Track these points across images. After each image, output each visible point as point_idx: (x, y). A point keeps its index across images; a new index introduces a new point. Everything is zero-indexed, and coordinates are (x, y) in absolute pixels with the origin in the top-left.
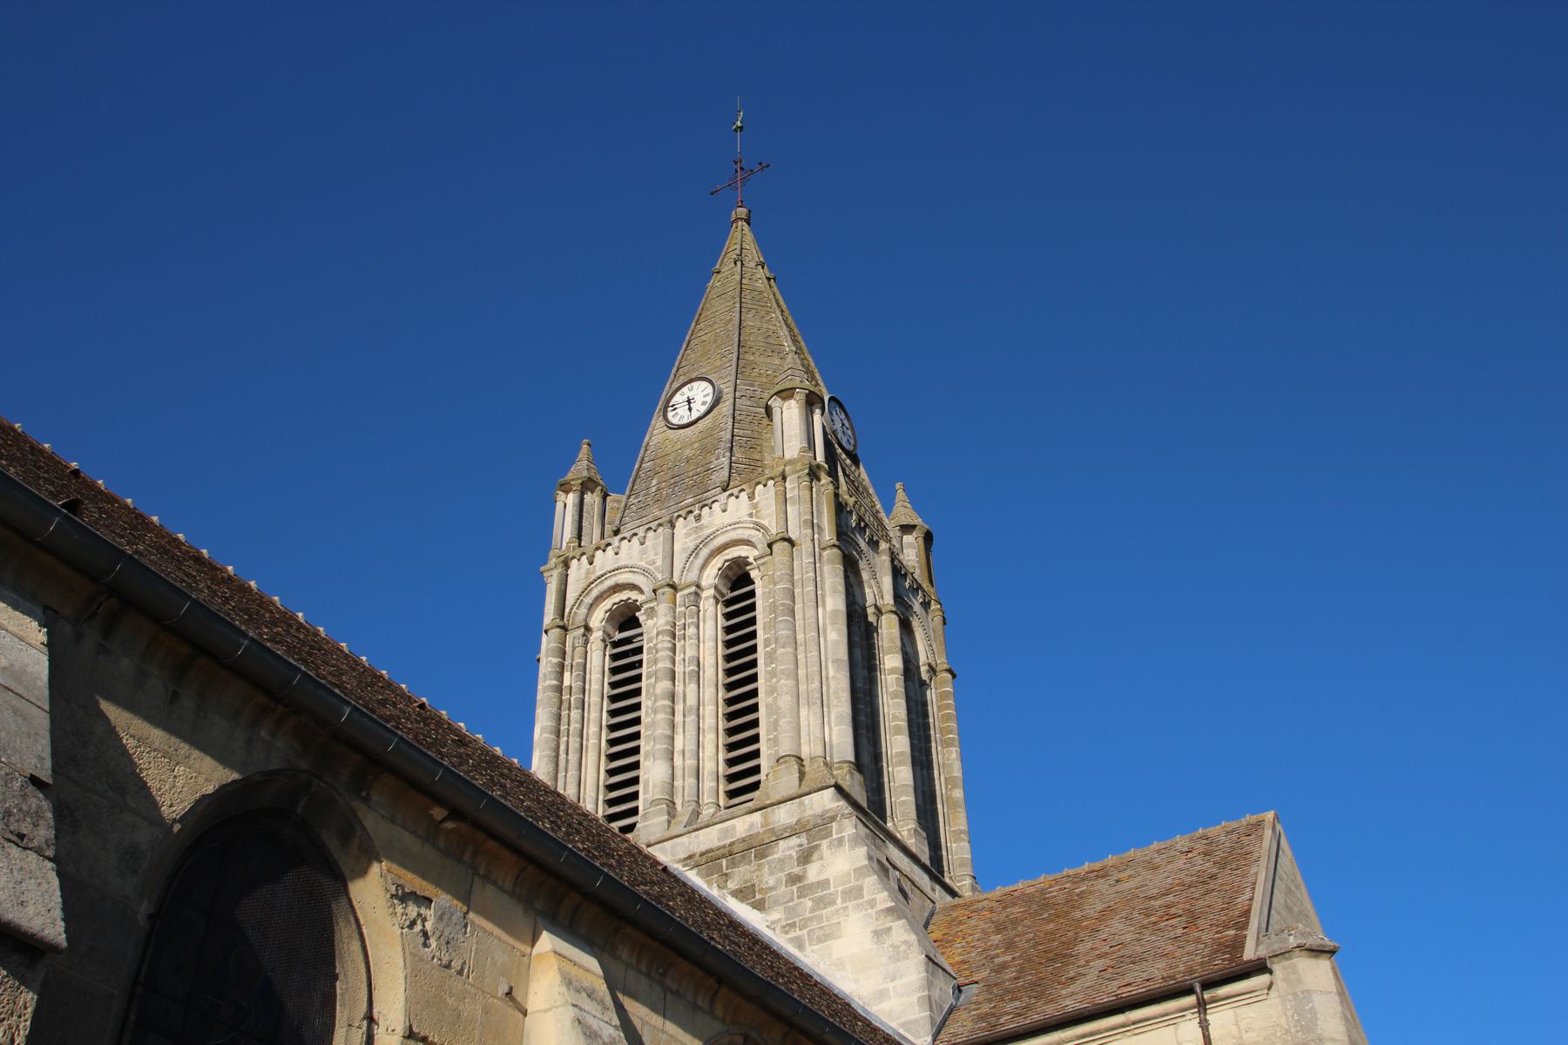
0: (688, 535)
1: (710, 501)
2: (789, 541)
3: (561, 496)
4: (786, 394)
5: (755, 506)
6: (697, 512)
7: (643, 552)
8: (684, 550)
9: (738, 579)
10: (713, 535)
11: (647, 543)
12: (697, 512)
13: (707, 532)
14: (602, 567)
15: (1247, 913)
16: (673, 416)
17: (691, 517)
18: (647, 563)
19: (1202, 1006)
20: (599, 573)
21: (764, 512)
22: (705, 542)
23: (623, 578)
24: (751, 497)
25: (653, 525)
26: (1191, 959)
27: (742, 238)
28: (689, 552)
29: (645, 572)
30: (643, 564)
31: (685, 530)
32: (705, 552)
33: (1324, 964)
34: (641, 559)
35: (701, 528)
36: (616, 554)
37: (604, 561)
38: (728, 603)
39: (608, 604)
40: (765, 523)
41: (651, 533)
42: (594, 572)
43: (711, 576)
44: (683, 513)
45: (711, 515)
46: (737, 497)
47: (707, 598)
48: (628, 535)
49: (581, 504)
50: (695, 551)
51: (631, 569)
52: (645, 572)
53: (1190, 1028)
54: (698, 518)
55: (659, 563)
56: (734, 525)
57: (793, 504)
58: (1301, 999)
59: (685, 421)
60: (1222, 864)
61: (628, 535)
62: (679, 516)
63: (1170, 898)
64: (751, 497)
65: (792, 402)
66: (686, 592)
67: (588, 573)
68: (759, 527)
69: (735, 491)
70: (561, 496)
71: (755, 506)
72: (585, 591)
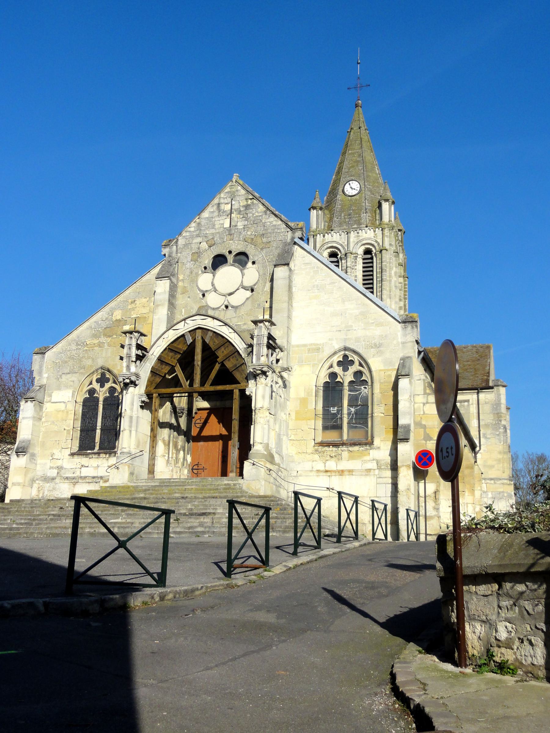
0: (355, 237)
2: (386, 250)
3: (312, 210)
4: (387, 200)
7: (341, 238)
8: (354, 242)
9: (368, 252)
10: (363, 240)
11: (342, 236)
13: (361, 238)
14: (328, 240)
15: (489, 373)
19: (478, 393)
20: (327, 241)
21: (378, 237)
22: (360, 241)
23: (334, 245)
25: (344, 231)
26: (478, 383)
27: (360, 115)
29: (341, 245)
30: (340, 242)
32: (360, 244)
33: (504, 388)
37: (328, 237)
38: (364, 259)
39: (329, 250)
40: (379, 241)
41: (343, 233)
42: (325, 240)
43: (361, 251)
45: (362, 233)
47: (359, 258)
49: (317, 216)
51: (337, 243)
52: (341, 245)
53: (475, 396)
54: (358, 233)
55: (346, 243)
56: (369, 239)
58: (499, 395)
59: (350, 194)
60: (481, 357)
63: (469, 363)
64: (375, 231)
65: (387, 203)
66: (355, 255)
67: (323, 240)
68: (376, 241)
69: (370, 228)
70: (312, 210)
71: (376, 235)
72: (323, 245)
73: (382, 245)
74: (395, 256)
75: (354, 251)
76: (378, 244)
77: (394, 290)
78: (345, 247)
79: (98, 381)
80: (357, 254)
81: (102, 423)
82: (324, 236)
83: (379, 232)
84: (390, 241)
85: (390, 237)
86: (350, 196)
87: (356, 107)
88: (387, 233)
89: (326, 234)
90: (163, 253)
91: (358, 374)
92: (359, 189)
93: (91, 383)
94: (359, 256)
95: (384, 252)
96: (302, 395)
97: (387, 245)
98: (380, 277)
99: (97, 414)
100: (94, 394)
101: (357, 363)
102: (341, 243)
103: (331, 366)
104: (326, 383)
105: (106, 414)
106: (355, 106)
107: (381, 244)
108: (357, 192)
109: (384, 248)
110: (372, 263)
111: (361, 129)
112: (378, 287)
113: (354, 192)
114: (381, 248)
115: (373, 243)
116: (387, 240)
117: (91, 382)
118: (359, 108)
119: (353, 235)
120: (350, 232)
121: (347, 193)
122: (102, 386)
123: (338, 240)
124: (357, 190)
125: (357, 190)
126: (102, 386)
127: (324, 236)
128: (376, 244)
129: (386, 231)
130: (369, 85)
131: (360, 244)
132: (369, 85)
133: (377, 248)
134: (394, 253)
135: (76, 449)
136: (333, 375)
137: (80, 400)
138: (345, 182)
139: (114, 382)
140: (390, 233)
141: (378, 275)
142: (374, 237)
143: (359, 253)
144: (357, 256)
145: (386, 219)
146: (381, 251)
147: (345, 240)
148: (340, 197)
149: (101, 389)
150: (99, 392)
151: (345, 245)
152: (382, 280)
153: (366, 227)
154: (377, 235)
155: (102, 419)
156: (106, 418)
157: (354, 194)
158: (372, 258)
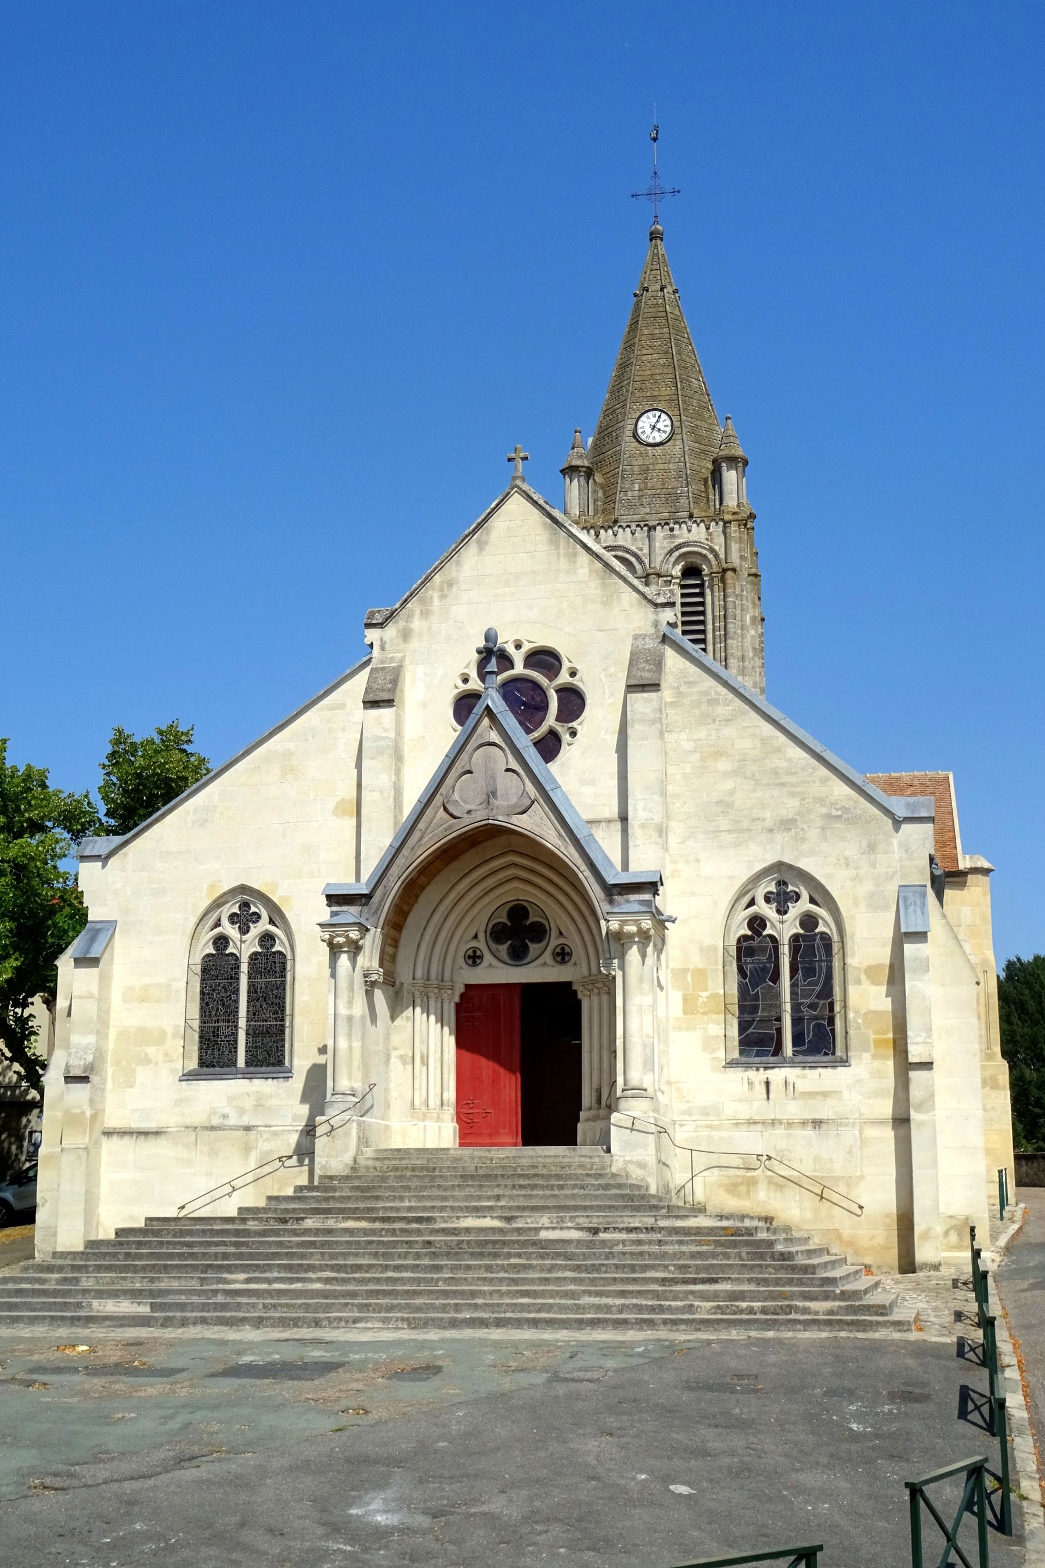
0: (665, 538)
1: (681, 520)
2: (734, 570)
5: (710, 534)
6: (672, 525)
7: (635, 540)
8: (663, 548)
9: (691, 571)
11: (637, 534)
12: (672, 525)
16: (642, 433)
17: (667, 527)
18: (637, 548)
21: (716, 540)
22: (678, 547)
24: (708, 529)
25: (642, 524)
28: (666, 551)
29: (635, 555)
30: (634, 548)
31: (662, 534)
32: (676, 554)
34: (633, 545)
35: (673, 536)
36: (615, 535)
38: (683, 587)
40: (717, 548)
41: (639, 529)
43: (677, 571)
44: (663, 523)
46: (698, 525)
48: (624, 525)
50: (671, 552)
51: (627, 551)
54: (672, 530)
55: (646, 551)
56: (695, 543)
57: (736, 543)
59: (651, 441)
61: (624, 525)
62: (659, 524)
64: (708, 529)
66: (665, 579)
68: (712, 550)
69: (698, 520)
71: (710, 534)
73: (726, 560)
74: (751, 583)
75: (663, 571)
76: (716, 556)
77: (751, 655)
78: (644, 559)
79: (233, 918)
80: (671, 576)
81: (248, 1011)
82: (597, 535)
83: (716, 529)
84: (740, 550)
85: (741, 541)
86: (649, 445)
87: (651, 240)
88: (735, 531)
89: (602, 531)
90: (367, 641)
91: (809, 921)
92: (668, 429)
93: (218, 924)
94: (673, 581)
95: (729, 574)
96: (697, 961)
97: (735, 560)
98: (722, 628)
99: (237, 991)
100: (226, 947)
101: (805, 895)
102: (636, 550)
103: (752, 903)
104: (745, 938)
105: (256, 992)
106: (648, 237)
107: (722, 556)
108: (664, 436)
109: (729, 566)
110: (702, 594)
111: (665, 290)
112: (718, 650)
113: (658, 437)
114: (725, 566)
115: (704, 552)
116: (734, 547)
117: (219, 920)
118: (659, 242)
119: (660, 533)
120: (655, 529)
121: (643, 437)
122: (244, 930)
123: (628, 545)
124: (665, 432)
125: (665, 432)
126: (244, 930)
127: (597, 535)
128: (711, 556)
129: (733, 528)
130: (679, 192)
131: (676, 554)
132: (679, 192)
133: (714, 562)
134: (749, 575)
135: (193, 1064)
136: (757, 923)
137: (197, 959)
138: (638, 414)
139: (272, 922)
140: (740, 532)
141: (717, 624)
142: (707, 539)
143: (674, 573)
144: (670, 581)
145: (731, 501)
146: (725, 571)
147: (643, 544)
148: (628, 444)
149: (245, 937)
150: (238, 943)
151: (644, 554)
152: (725, 635)
153: (691, 516)
154: (715, 534)
155: (248, 1002)
156: (258, 1000)
157: (658, 440)
158: (701, 586)
